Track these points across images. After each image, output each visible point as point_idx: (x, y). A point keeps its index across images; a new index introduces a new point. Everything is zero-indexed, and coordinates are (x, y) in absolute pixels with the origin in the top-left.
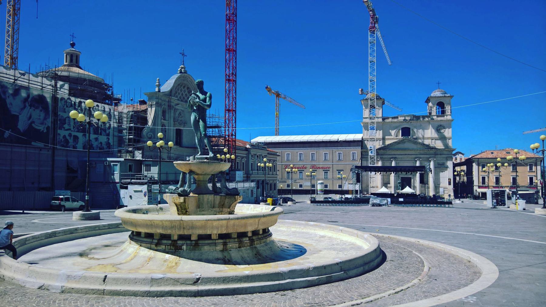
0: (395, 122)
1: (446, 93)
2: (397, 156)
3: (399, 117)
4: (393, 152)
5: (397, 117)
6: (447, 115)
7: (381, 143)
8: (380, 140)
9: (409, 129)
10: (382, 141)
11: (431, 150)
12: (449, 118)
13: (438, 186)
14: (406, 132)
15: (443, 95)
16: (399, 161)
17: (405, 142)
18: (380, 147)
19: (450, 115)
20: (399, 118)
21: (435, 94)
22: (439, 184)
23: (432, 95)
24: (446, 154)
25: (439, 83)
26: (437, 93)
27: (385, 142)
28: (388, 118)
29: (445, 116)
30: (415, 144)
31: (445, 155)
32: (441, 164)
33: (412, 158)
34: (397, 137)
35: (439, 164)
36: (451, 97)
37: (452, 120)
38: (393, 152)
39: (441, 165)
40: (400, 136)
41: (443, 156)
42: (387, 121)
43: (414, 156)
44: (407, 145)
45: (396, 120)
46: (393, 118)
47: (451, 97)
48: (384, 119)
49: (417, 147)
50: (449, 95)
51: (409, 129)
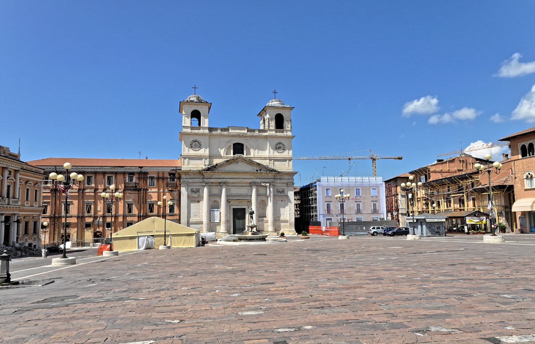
0: (225, 136)
1: (284, 104)
2: (228, 180)
3: (230, 130)
4: (223, 176)
5: (227, 130)
6: (287, 131)
7: (207, 163)
8: (206, 159)
9: (242, 145)
10: (208, 159)
11: (269, 173)
12: (289, 134)
13: (278, 219)
14: (238, 148)
15: (283, 106)
16: (230, 187)
17: (238, 162)
18: (207, 167)
19: (291, 131)
20: (230, 131)
21: (270, 103)
22: (278, 216)
23: (270, 104)
24: (287, 178)
25: (275, 92)
26: (275, 103)
27: (213, 162)
28: (216, 129)
29: (285, 133)
30: (250, 164)
31: (285, 180)
32: (281, 191)
33: (246, 183)
34: (228, 156)
35: (278, 192)
36: (292, 108)
37: (293, 137)
38: (223, 176)
39: (281, 192)
40: (232, 155)
41: (283, 181)
42: (214, 132)
43: (249, 181)
44: (241, 167)
45: (226, 133)
46: (222, 130)
47: (292, 108)
48: (211, 129)
49: (253, 169)
50: (289, 106)
51: (242, 145)
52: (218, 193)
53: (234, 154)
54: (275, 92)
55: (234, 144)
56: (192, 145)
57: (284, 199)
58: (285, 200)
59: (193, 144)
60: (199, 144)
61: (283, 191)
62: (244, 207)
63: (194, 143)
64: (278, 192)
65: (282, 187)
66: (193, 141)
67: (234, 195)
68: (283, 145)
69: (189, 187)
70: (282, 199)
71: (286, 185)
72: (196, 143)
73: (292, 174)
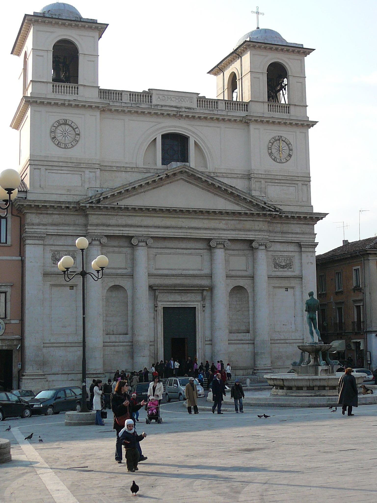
39: (283, 267)
52: (124, 266)
53: (165, 161)
54: (258, 13)
55: (162, 135)
56: (54, 132)
57: (292, 285)
58: (293, 288)
59: (58, 131)
60: (73, 132)
61: (288, 266)
62: (191, 305)
63: (60, 128)
64: (277, 265)
65: (286, 254)
66: (58, 121)
67: (166, 272)
68: (288, 144)
69: (48, 248)
70: (288, 285)
71: (296, 249)
72: (67, 127)
73: (311, 218)
